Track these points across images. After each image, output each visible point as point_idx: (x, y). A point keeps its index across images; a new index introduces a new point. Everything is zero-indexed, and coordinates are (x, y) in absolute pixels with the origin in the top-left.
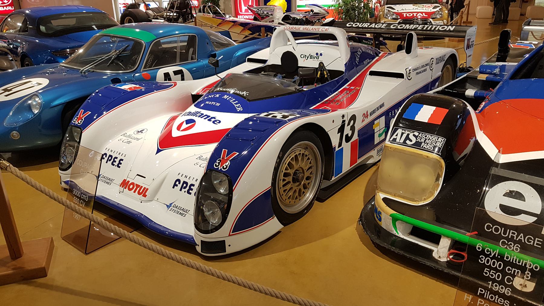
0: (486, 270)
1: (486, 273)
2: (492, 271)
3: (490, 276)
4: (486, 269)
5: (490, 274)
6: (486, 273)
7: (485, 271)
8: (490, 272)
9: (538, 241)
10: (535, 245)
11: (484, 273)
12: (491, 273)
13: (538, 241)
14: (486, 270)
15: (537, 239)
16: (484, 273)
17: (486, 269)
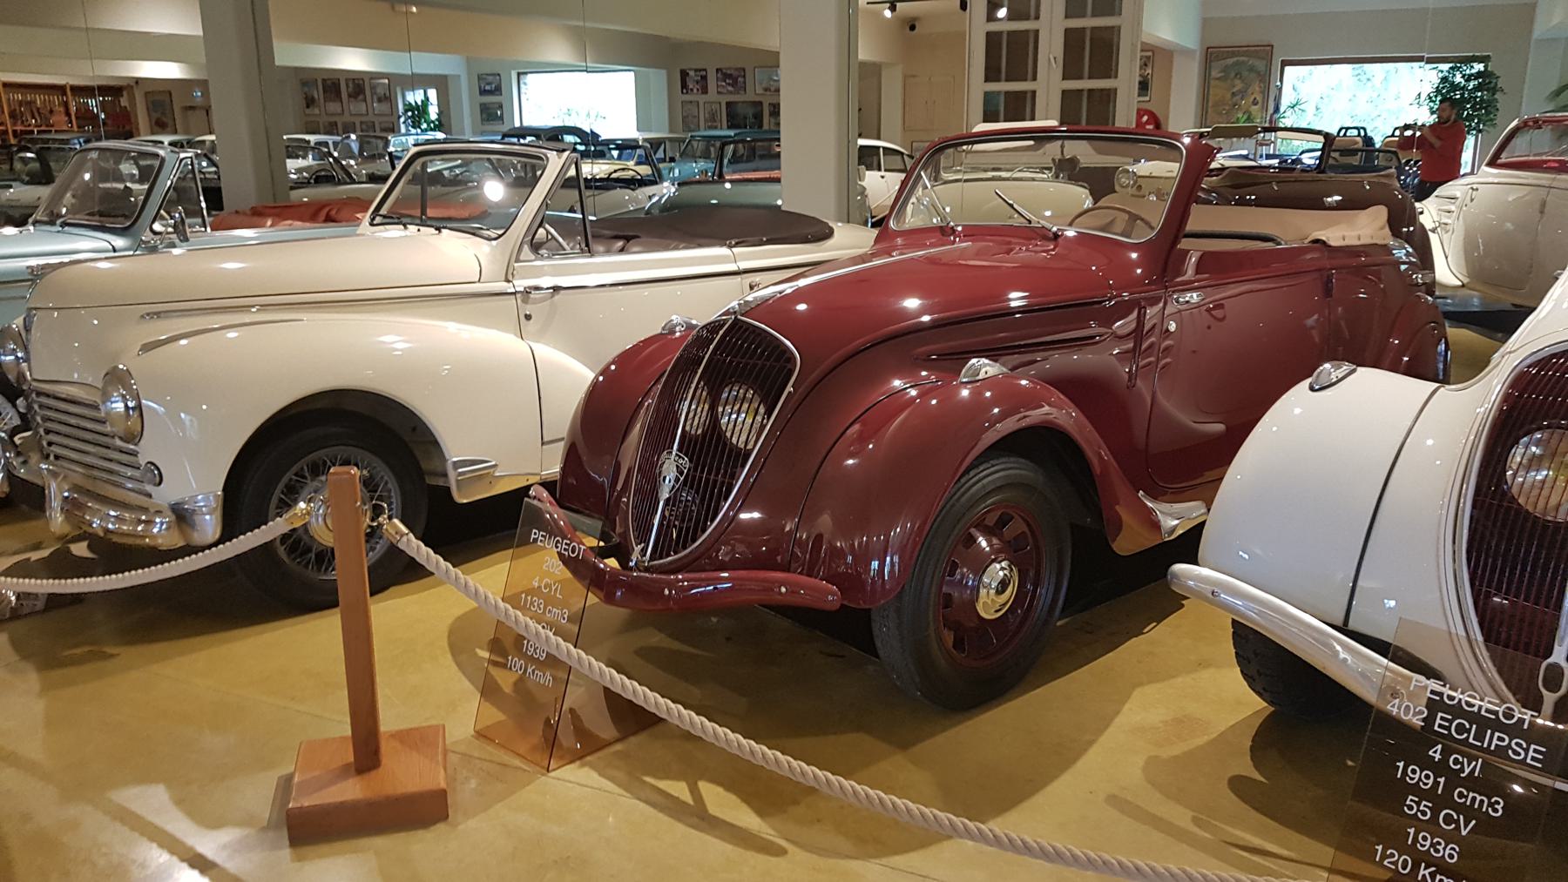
0: (1411, 800)
1: (1411, 808)
2: (1424, 803)
3: (1419, 814)
4: (1410, 797)
5: (1418, 810)
6: (1411, 808)
7: (1408, 802)
8: (1418, 804)
9: (1535, 751)
10: (1529, 761)
11: (1405, 808)
12: (1422, 808)
13: (1535, 751)
14: (1411, 800)
15: (1533, 747)
16: (1405, 808)
17: (1410, 797)
